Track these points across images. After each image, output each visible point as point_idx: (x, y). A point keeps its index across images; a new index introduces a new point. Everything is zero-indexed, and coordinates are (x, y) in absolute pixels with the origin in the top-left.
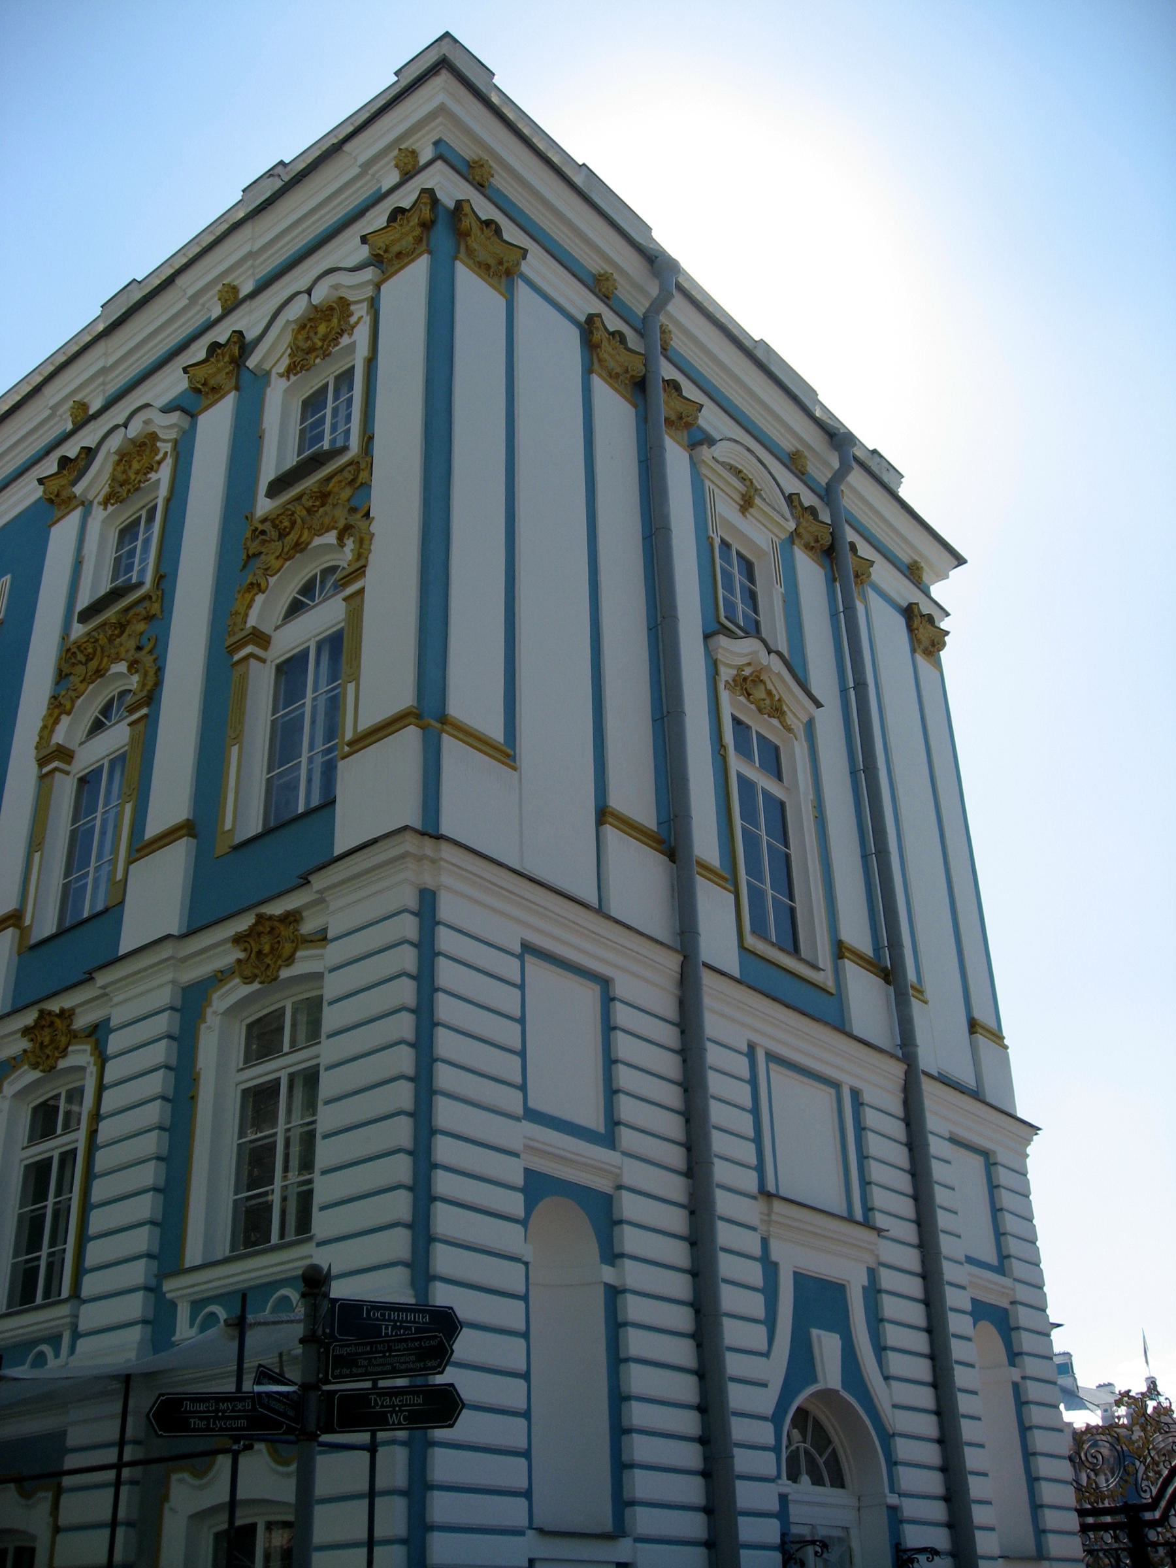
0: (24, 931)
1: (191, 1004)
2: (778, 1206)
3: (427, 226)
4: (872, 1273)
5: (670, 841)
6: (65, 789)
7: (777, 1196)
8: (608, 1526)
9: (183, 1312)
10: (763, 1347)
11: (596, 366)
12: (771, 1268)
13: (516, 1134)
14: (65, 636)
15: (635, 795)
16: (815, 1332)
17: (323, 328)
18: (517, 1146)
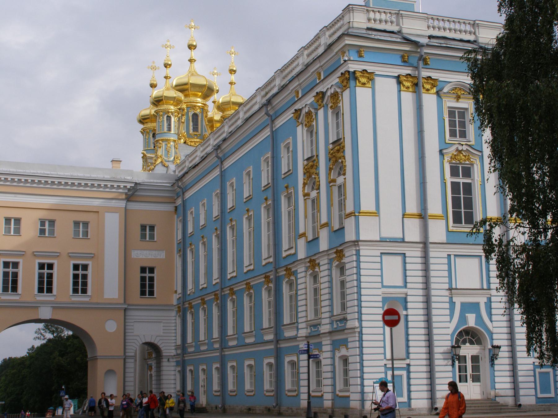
0: (307, 238)
1: (330, 262)
2: (453, 291)
3: (348, 79)
4: (489, 300)
5: (423, 216)
6: (309, 202)
7: (456, 289)
8: (405, 357)
9: (335, 322)
10: (449, 320)
11: (402, 88)
12: (452, 304)
13: (379, 292)
14: (304, 164)
15: (412, 207)
16: (467, 315)
17: (335, 96)
18: (380, 294)
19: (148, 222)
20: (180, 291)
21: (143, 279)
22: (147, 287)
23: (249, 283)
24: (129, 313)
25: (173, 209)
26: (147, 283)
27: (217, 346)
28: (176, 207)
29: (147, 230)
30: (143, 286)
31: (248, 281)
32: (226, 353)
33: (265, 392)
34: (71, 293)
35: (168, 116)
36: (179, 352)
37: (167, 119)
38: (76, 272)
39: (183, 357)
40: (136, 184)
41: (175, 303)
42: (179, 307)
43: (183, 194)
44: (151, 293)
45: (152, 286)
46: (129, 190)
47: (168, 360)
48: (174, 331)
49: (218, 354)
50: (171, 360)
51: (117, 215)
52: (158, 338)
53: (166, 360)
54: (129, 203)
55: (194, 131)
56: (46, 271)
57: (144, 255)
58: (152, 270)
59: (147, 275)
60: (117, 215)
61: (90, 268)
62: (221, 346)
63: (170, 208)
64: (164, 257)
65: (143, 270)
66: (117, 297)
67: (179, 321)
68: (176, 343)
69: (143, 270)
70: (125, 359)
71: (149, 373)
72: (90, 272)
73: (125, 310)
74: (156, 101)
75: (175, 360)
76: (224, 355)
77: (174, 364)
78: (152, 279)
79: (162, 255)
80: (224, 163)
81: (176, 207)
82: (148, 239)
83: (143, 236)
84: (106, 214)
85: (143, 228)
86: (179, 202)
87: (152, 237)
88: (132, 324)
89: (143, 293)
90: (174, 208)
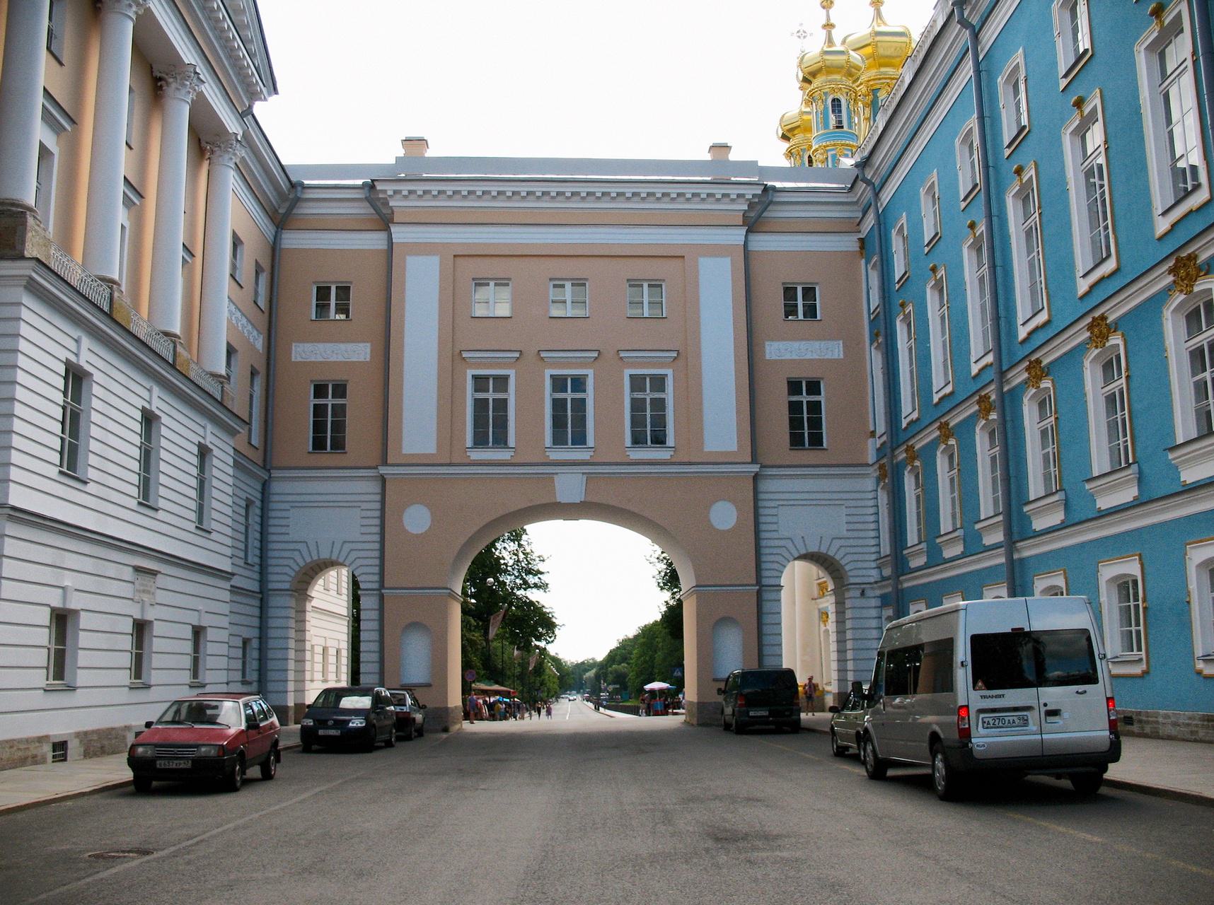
19: (800, 278)
20: (881, 428)
21: (795, 408)
22: (805, 428)
23: (1103, 318)
24: (765, 485)
25: (855, 246)
26: (805, 416)
27: (998, 537)
28: (862, 241)
29: (800, 302)
30: (795, 423)
31: (1097, 314)
32: (1026, 554)
33: (1200, 665)
34: (628, 442)
35: (834, 100)
36: (887, 572)
38: (639, 395)
39: (898, 582)
40: (766, 189)
41: (871, 457)
42: (882, 467)
44: (816, 441)
45: (816, 423)
47: (863, 593)
48: (873, 526)
49: (1003, 560)
50: (869, 593)
52: (837, 543)
53: (858, 593)
54: (752, 237)
56: (569, 395)
57: (792, 350)
58: (814, 387)
59: (805, 398)
60: (726, 263)
61: (670, 383)
62: (1009, 533)
63: (849, 243)
64: (842, 356)
65: (794, 387)
66: (733, 447)
67: (883, 498)
68: (879, 552)
69: (794, 387)
70: (759, 593)
71: (823, 628)
72: (669, 395)
73: (756, 477)
74: (810, 73)
75: (878, 592)
76: (1021, 560)
77: (875, 602)
78: (815, 407)
79: (835, 350)
80: (981, 36)
81: (862, 241)
82: (801, 316)
83: (790, 310)
84: (701, 260)
85: (789, 292)
87: (811, 312)
88: (773, 511)
89: (796, 441)
90: (858, 244)
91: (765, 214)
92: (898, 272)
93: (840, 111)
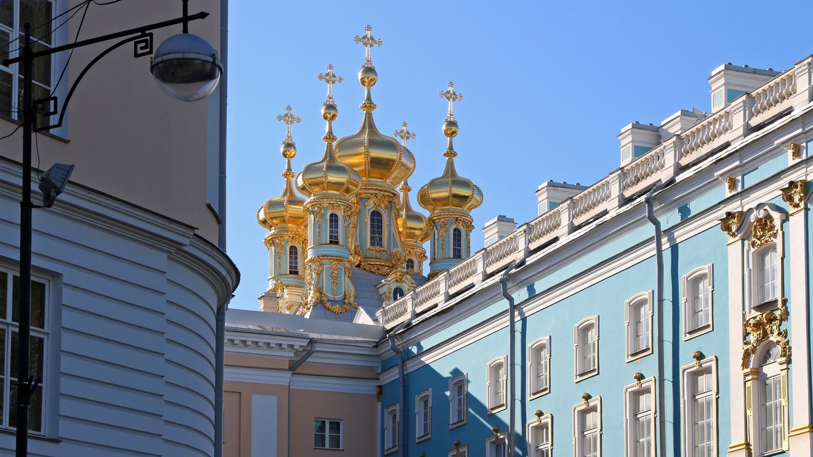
19: (329, 415)
25: (375, 392)
28: (380, 387)
37: (331, 221)
40: (312, 341)
43: (403, 362)
46: (297, 352)
51: (274, 399)
55: (372, 244)
60: (274, 399)
63: (368, 388)
86: (394, 374)
87: (335, 442)
90: (377, 390)
91: (309, 360)
92: (419, 432)
93: (337, 227)
